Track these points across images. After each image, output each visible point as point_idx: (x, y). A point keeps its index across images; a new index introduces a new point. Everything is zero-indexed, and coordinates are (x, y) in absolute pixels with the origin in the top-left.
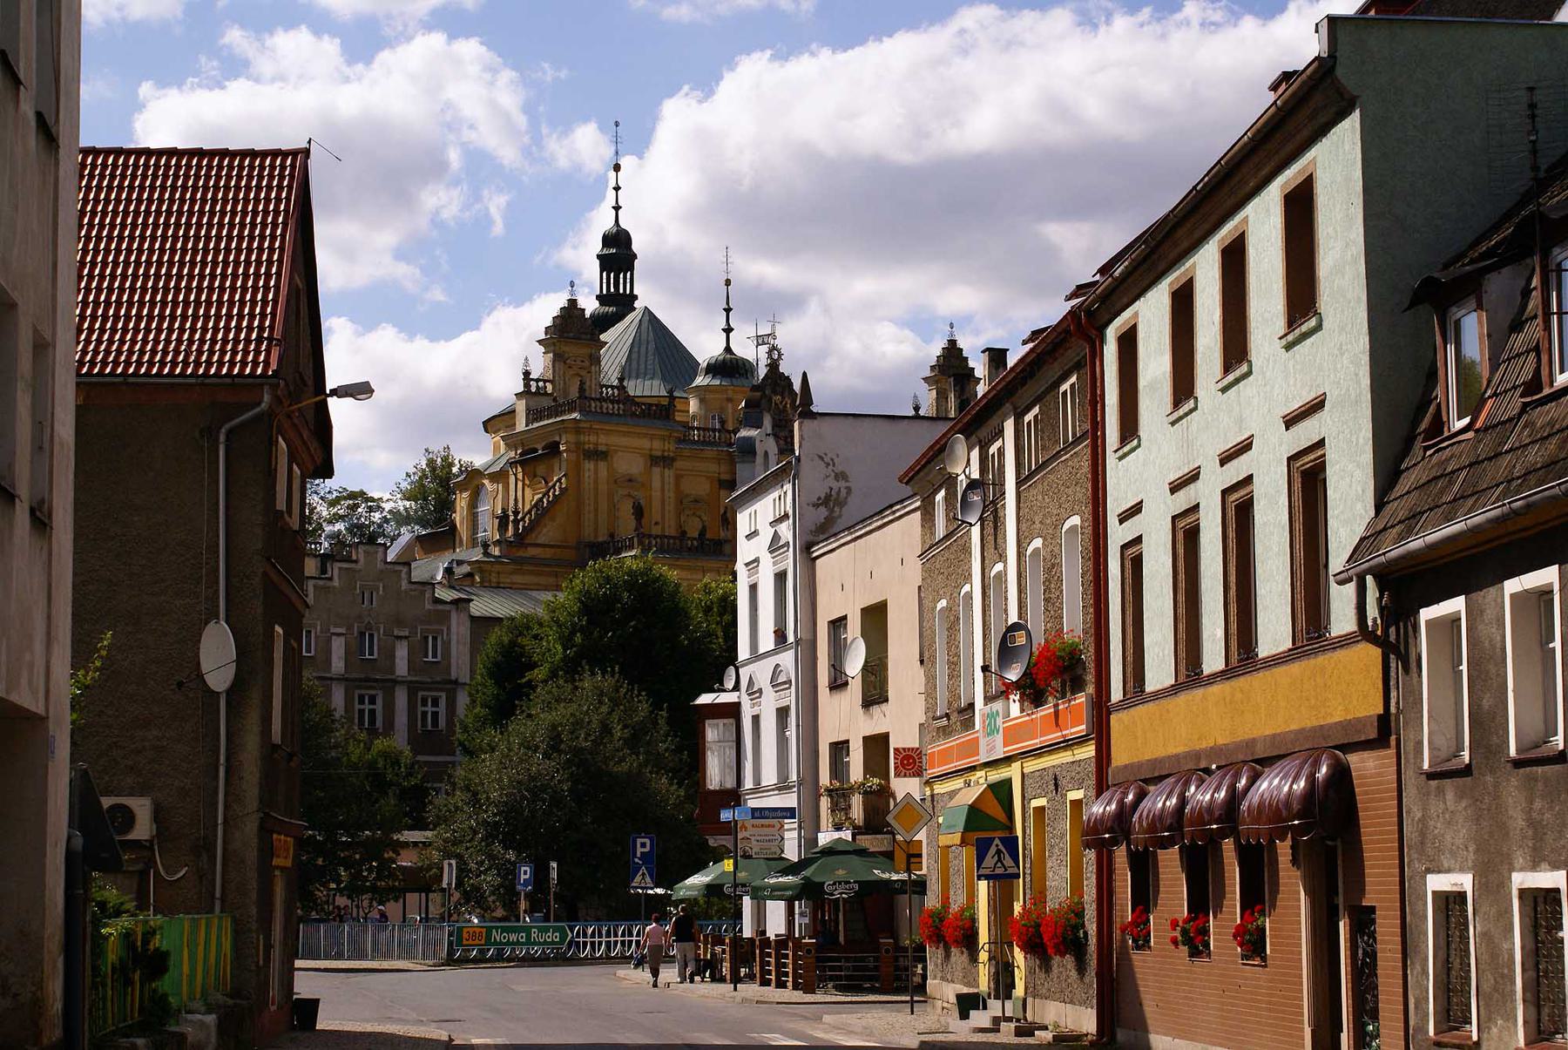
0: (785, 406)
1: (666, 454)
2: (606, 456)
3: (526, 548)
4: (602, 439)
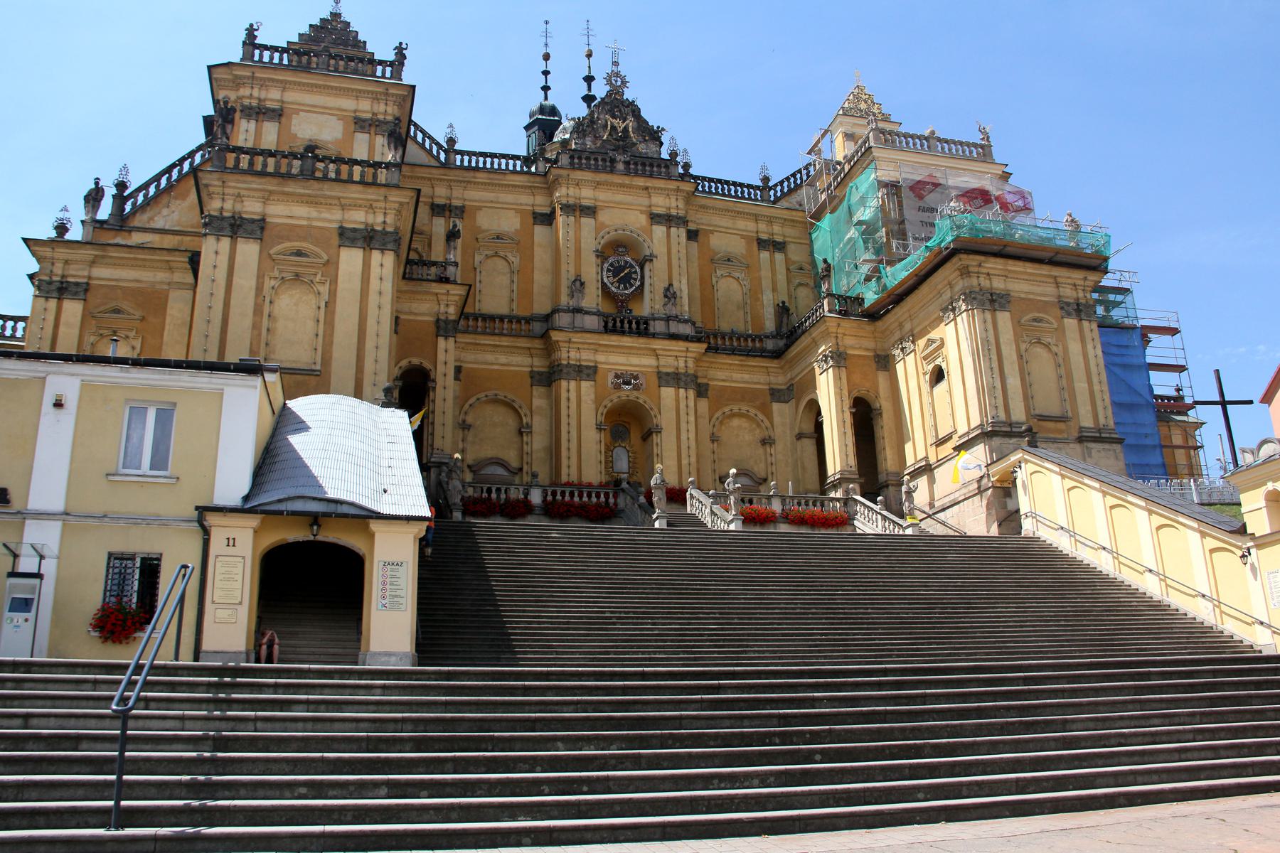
0: (626, 130)
1: (381, 117)
2: (280, 115)
3: (130, 231)
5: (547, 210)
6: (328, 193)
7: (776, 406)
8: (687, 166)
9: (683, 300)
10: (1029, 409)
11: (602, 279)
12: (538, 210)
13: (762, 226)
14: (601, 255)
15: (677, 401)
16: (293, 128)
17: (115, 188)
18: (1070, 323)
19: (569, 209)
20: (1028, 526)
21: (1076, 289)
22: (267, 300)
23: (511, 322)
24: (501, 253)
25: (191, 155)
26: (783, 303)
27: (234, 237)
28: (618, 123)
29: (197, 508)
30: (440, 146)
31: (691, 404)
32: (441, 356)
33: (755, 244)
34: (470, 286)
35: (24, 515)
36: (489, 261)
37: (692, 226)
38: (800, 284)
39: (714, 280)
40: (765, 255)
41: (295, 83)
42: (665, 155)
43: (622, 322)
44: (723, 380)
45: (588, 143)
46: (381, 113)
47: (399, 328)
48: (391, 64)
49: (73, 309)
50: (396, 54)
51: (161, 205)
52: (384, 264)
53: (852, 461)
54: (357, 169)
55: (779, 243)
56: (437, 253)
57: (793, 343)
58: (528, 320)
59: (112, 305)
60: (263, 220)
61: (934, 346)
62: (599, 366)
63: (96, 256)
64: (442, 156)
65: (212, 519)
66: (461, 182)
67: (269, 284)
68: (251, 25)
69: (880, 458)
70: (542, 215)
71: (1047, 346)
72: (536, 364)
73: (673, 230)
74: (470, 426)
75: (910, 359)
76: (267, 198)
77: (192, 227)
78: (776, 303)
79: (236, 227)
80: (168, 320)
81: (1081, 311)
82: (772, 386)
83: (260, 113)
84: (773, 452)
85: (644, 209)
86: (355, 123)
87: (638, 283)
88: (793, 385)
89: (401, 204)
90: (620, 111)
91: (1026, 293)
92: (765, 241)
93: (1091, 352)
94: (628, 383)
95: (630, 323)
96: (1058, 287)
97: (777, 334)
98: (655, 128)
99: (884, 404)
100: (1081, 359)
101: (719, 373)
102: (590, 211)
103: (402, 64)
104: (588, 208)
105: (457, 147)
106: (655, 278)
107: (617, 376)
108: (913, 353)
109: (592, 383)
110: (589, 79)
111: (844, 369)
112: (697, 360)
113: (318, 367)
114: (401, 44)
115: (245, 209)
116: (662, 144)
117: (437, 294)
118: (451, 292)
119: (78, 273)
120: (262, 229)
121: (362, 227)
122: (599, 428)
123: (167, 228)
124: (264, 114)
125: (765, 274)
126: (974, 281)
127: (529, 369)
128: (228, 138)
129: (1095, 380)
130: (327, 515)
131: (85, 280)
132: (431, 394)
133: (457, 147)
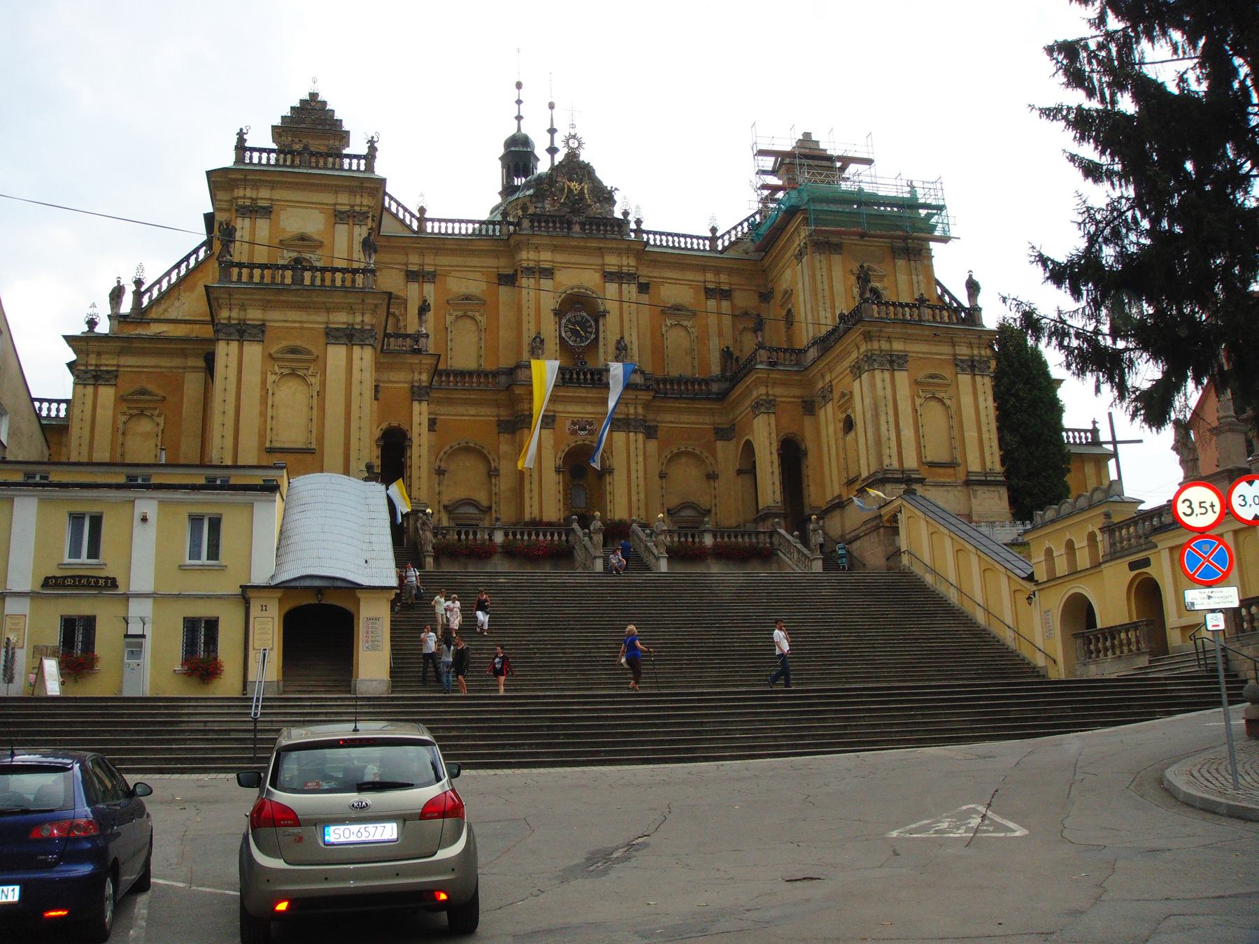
0: (582, 189)
1: (357, 209)
3: (149, 323)
4: (265, 193)
5: (511, 272)
6: (315, 299)
7: (719, 444)
8: (638, 222)
9: (633, 351)
10: (921, 456)
11: (560, 334)
12: (502, 271)
13: (710, 276)
14: (558, 313)
15: (628, 444)
16: (281, 222)
17: (134, 285)
18: (964, 379)
19: (530, 271)
20: (905, 560)
21: (972, 348)
22: (270, 392)
23: (479, 375)
24: (470, 313)
25: (196, 251)
26: (728, 348)
27: (241, 341)
28: (575, 186)
29: (241, 587)
30: (412, 215)
31: (640, 445)
32: (416, 419)
33: (703, 293)
34: (440, 355)
35: (127, 597)
36: (461, 322)
37: (642, 280)
38: (745, 329)
39: (664, 329)
40: (712, 304)
41: (282, 182)
42: (618, 214)
43: (578, 374)
44: (672, 422)
45: (547, 206)
46: (357, 205)
47: (380, 395)
48: (365, 157)
49: (107, 394)
50: (369, 147)
51: (172, 298)
52: (364, 357)
53: (778, 497)
54: (339, 276)
55: (727, 291)
56: (412, 324)
57: (734, 386)
58: (495, 374)
59: (137, 387)
60: (264, 325)
61: (846, 398)
62: (557, 414)
63: (122, 347)
64: (415, 225)
65: (250, 594)
66: (432, 249)
67: (271, 378)
68: (241, 130)
69: (806, 493)
70: (507, 276)
71: (941, 401)
72: (502, 413)
73: (625, 286)
74: (445, 471)
75: (829, 407)
76: (266, 305)
77: (201, 316)
78: (722, 347)
79: (243, 332)
80: (185, 400)
81: (975, 366)
82: (717, 426)
83: (254, 211)
84: (716, 485)
85: (599, 267)
86: (336, 215)
87: (593, 336)
88: (734, 425)
89: (376, 305)
90: (577, 173)
91: (924, 353)
92: (713, 289)
93: (982, 405)
94: (584, 429)
95: (585, 374)
96: (954, 346)
97: (722, 377)
98: (609, 189)
99: (810, 445)
100: (973, 411)
101: (668, 416)
102: (548, 273)
103: (374, 157)
104: (547, 270)
105: (427, 216)
106: (610, 331)
107: (574, 423)
108: (831, 403)
109: (552, 430)
110: (552, 131)
111: (773, 415)
112: (647, 406)
113: (313, 447)
114: (373, 137)
115: (248, 317)
116: (615, 202)
117: (411, 364)
118: (424, 361)
119: (109, 362)
120: (263, 332)
121: (345, 326)
122: (558, 471)
123: (179, 318)
124: (257, 211)
125: (712, 320)
126: (876, 345)
127: (497, 419)
128: (231, 256)
129: (984, 429)
130: (328, 588)
131: (114, 368)
132: (408, 451)
133: (427, 216)
